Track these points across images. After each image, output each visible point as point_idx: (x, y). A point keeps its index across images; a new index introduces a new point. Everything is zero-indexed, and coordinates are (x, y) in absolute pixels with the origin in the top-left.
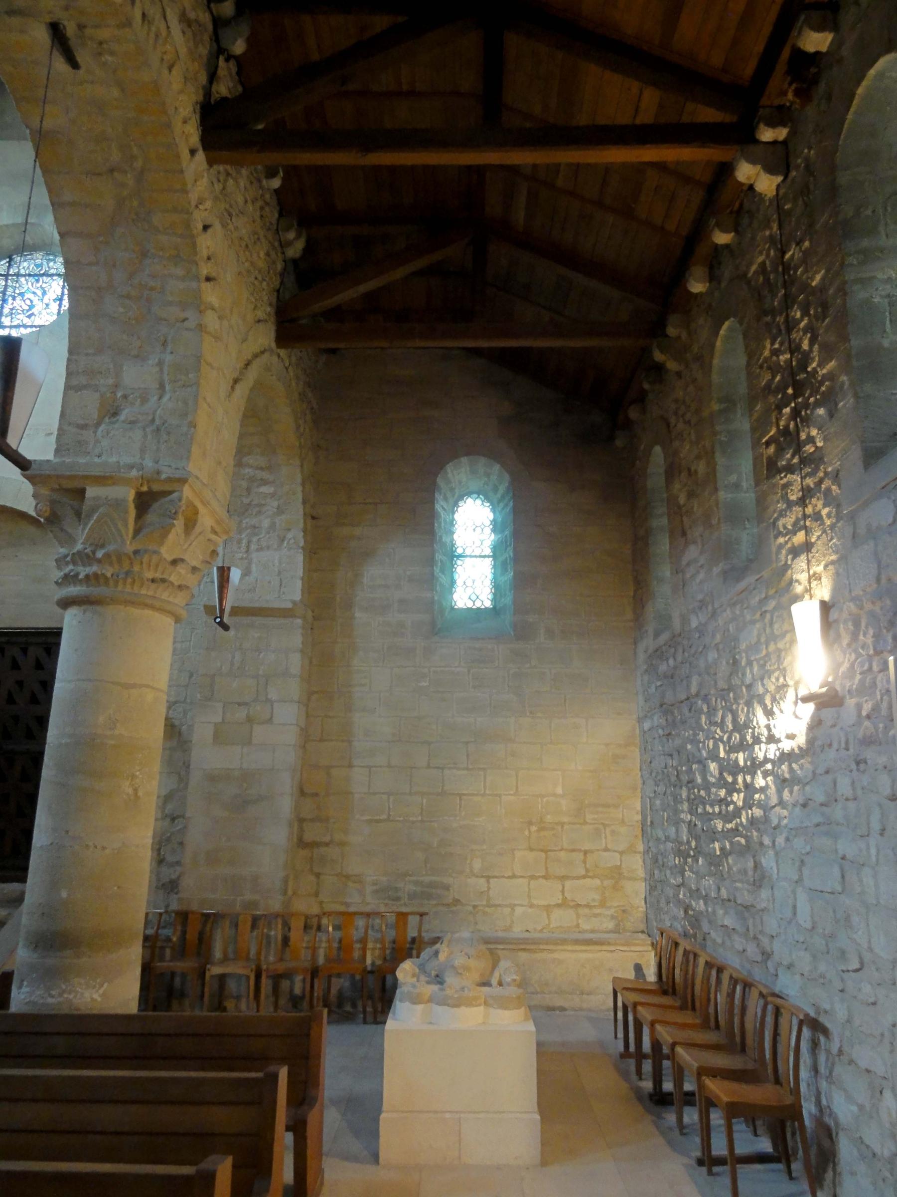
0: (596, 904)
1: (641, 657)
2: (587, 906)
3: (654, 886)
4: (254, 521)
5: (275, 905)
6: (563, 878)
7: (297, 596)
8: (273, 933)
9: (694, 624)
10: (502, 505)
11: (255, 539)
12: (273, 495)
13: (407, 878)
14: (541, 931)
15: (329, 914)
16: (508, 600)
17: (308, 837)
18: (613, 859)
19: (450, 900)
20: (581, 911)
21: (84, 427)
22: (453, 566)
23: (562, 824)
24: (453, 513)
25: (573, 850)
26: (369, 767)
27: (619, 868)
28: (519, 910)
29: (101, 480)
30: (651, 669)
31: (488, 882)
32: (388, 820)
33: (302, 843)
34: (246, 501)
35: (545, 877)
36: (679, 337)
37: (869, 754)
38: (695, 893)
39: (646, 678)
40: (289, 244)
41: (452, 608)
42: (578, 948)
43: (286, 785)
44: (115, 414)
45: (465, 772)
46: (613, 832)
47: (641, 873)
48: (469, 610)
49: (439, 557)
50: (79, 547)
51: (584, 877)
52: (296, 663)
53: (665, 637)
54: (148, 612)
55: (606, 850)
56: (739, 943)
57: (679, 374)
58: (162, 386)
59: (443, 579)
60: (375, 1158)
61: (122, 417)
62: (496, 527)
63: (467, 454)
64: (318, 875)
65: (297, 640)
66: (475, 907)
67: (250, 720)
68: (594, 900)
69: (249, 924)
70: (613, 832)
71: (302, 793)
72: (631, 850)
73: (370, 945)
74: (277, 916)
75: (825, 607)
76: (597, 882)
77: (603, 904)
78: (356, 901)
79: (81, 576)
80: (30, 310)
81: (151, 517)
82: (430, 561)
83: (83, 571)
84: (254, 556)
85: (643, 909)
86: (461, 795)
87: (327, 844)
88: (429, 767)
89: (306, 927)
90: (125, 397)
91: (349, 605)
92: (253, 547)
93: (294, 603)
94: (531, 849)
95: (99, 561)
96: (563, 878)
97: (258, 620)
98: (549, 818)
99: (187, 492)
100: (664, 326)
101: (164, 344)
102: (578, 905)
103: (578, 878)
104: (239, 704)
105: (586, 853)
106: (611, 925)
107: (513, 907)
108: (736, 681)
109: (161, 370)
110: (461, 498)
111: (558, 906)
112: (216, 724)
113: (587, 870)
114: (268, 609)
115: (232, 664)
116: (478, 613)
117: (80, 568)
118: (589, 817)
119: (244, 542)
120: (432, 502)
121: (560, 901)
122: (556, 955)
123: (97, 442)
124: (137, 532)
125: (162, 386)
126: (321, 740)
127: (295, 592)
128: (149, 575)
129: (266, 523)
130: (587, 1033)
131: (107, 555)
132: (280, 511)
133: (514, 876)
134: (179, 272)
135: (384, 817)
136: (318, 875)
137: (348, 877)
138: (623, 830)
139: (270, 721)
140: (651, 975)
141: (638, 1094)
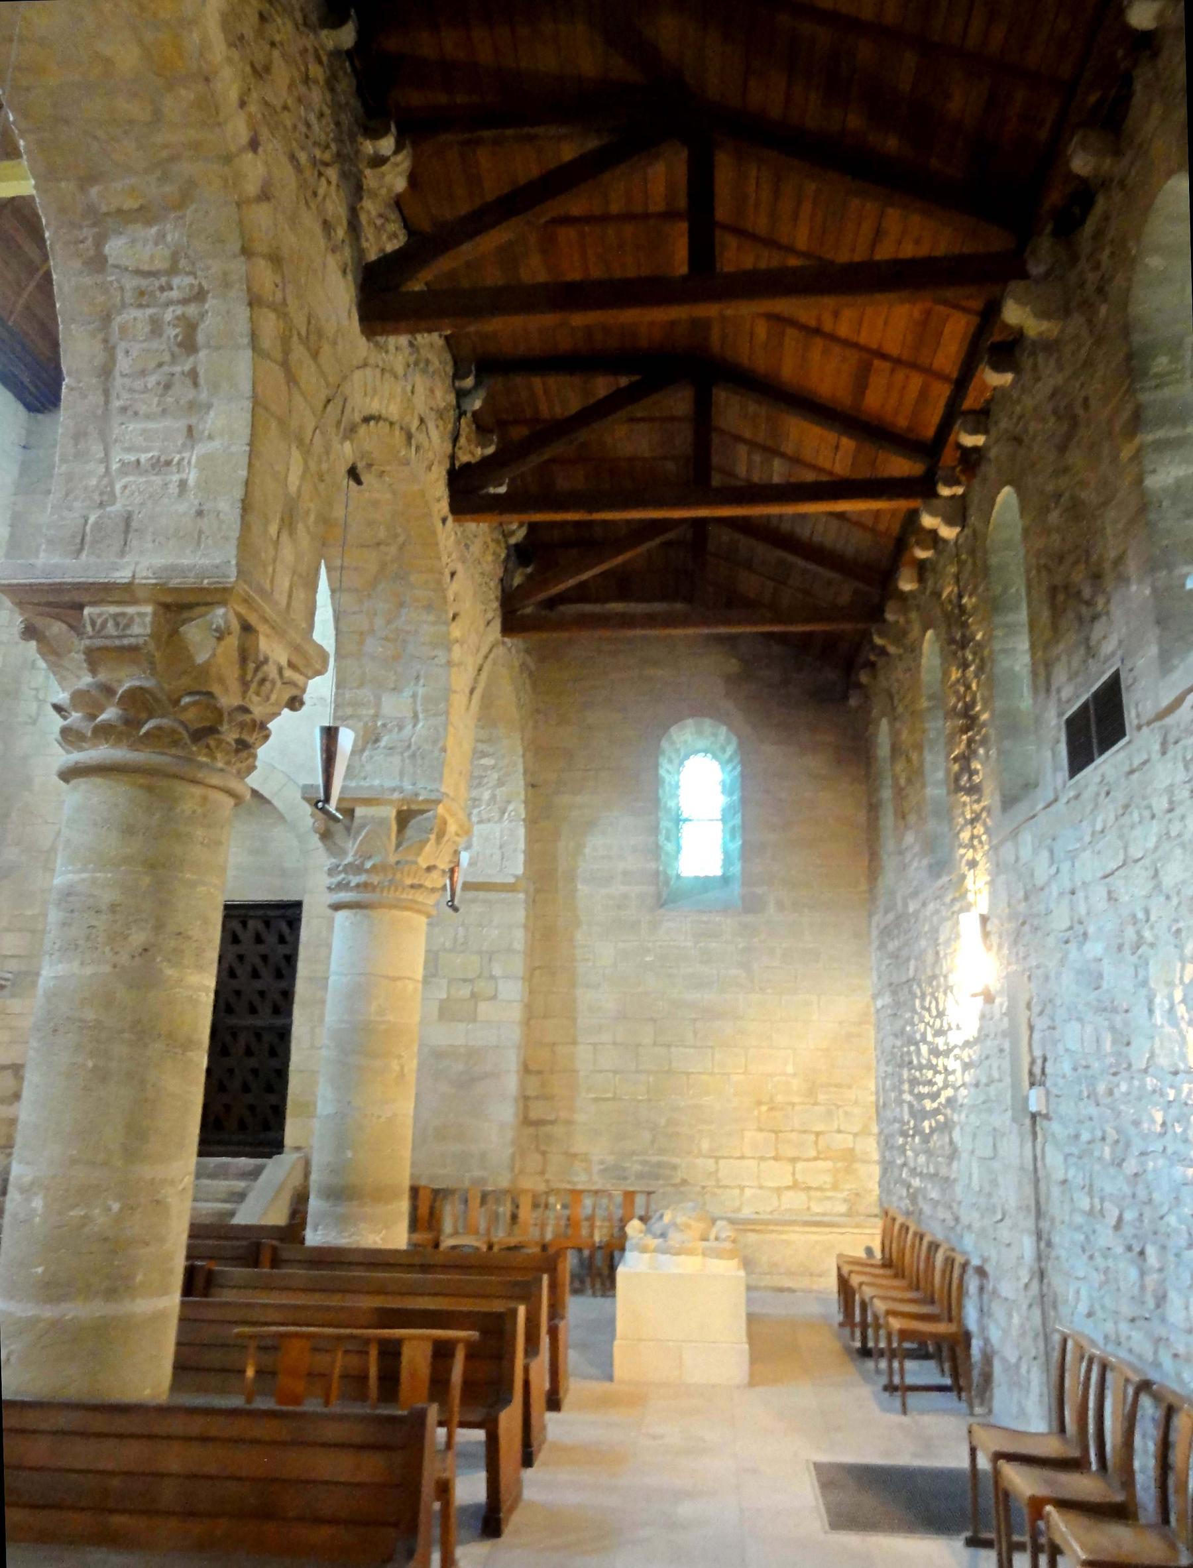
0: (828, 1186)
1: (875, 933)
2: (819, 1189)
3: (886, 1166)
5: (504, 1182)
6: (794, 1160)
7: (520, 870)
8: (501, 1209)
9: (911, 910)
10: (730, 767)
11: (475, 811)
12: (493, 767)
13: (635, 1158)
14: (771, 1212)
15: (556, 1192)
16: (737, 868)
17: (533, 1115)
19: (678, 1181)
20: (813, 1193)
22: (678, 831)
23: (793, 1105)
24: (679, 773)
25: (805, 1132)
26: (595, 1045)
27: (852, 1150)
28: (748, 1192)
29: (367, 802)
30: (882, 946)
31: (717, 1163)
32: (614, 1099)
33: (526, 1121)
35: (776, 1158)
36: (897, 622)
38: (914, 1172)
40: (512, 533)
41: (678, 876)
42: (807, 1229)
43: (511, 1062)
44: (377, 740)
45: (692, 1050)
46: (846, 1113)
47: (876, 1156)
48: (697, 878)
49: (665, 824)
50: (349, 859)
51: (816, 1159)
52: (519, 938)
53: (891, 916)
54: (406, 914)
55: (839, 1131)
56: (942, 1213)
57: (900, 657)
58: (415, 716)
59: (669, 847)
60: (610, 1378)
61: (383, 743)
62: (727, 790)
63: (692, 716)
64: (544, 1153)
65: (520, 915)
66: (704, 1187)
67: (474, 995)
68: (825, 1183)
69: (478, 1200)
70: (846, 1113)
72: (864, 1132)
73: (598, 1223)
74: (506, 1192)
75: (984, 919)
76: (829, 1164)
77: (835, 1187)
78: (581, 1181)
79: (352, 884)
81: (409, 832)
82: (655, 830)
83: (355, 880)
84: (477, 829)
85: (876, 1191)
86: (688, 1074)
87: (552, 1122)
88: (655, 1044)
89: (535, 1206)
90: (384, 725)
91: (571, 877)
93: (516, 877)
94: (760, 1130)
95: (367, 871)
96: (794, 1160)
97: (482, 895)
98: (780, 1098)
99: (440, 809)
100: (882, 611)
101: (418, 678)
102: (809, 1188)
103: (808, 1160)
104: (465, 980)
105: (818, 1134)
106: (843, 1208)
107: (742, 1188)
108: (937, 972)
109: (415, 702)
110: (687, 757)
111: (788, 1188)
112: (442, 1001)
113: (819, 1152)
114: (489, 884)
115: (455, 940)
116: (705, 884)
117: (351, 877)
118: (821, 1098)
120: (656, 766)
121: (791, 1184)
122: (784, 1237)
123: (363, 766)
124: (398, 845)
125: (415, 716)
126: (545, 1017)
127: (517, 866)
128: (408, 882)
129: (486, 795)
130: (814, 1309)
131: (374, 867)
132: (501, 783)
133: (742, 1157)
134: (431, 618)
135: (610, 1095)
136: (544, 1153)
137: (575, 1155)
138: (857, 1111)
139: (494, 997)
140: (878, 1254)
141: (848, 1350)
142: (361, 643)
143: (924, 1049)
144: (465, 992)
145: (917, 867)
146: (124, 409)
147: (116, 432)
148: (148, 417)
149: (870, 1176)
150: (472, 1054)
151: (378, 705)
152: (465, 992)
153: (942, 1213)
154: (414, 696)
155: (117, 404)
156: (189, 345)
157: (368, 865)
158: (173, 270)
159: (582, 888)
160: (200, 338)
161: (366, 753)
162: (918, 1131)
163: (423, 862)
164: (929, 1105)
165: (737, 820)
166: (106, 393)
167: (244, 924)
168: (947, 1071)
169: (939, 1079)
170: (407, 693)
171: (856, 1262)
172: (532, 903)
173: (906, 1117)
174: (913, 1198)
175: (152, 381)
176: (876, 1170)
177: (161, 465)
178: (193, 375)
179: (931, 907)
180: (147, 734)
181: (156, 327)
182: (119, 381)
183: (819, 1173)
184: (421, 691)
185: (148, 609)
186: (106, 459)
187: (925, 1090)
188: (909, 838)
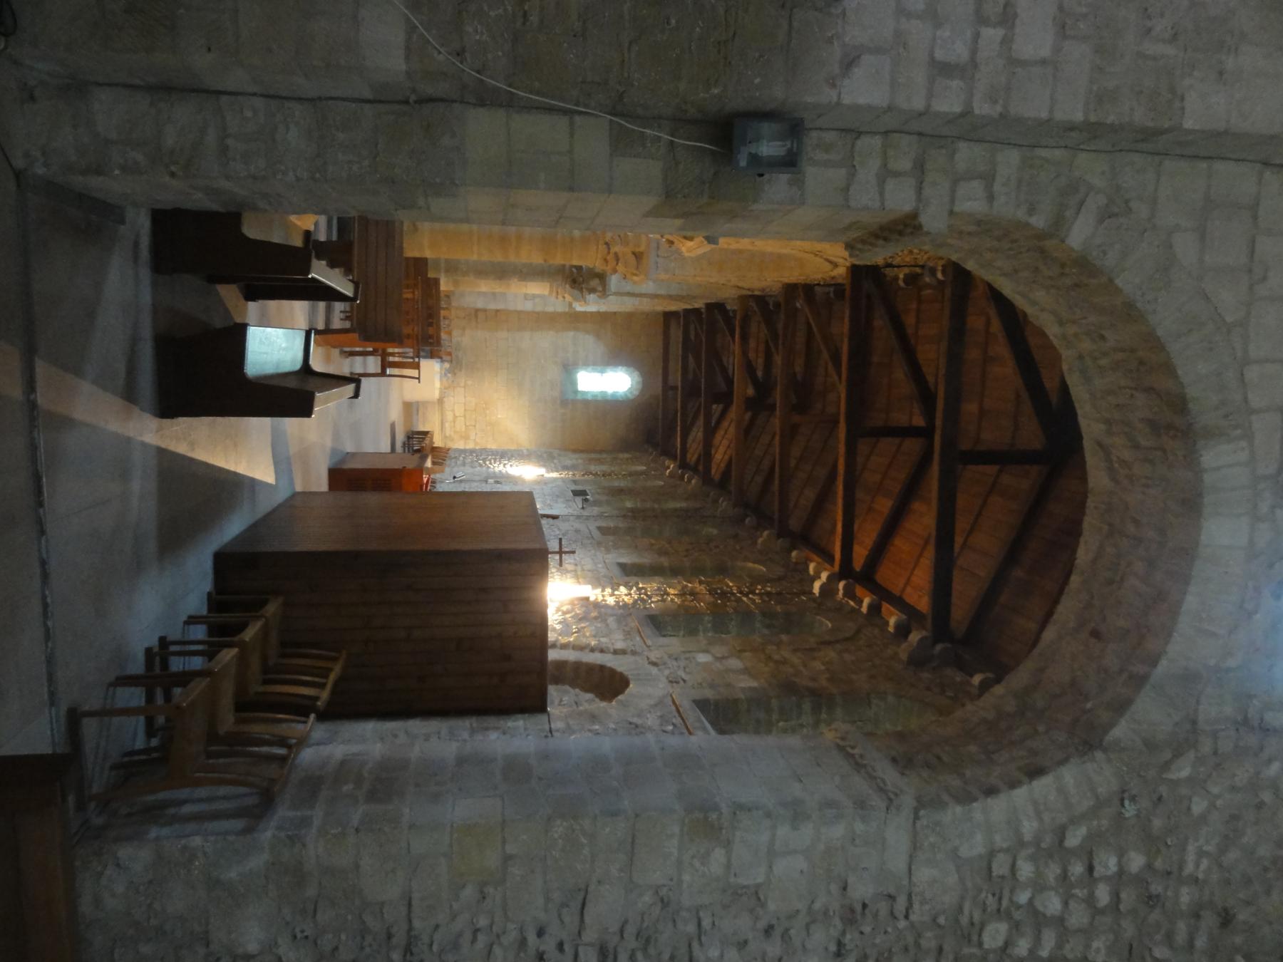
3: (464, 451)
5: (454, 304)
6: (465, 416)
16: (579, 397)
18: (473, 437)
19: (456, 371)
23: (486, 417)
33: (477, 310)
35: (465, 410)
43: (500, 306)
47: (467, 447)
49: (599, 368)
52: (550, 309)
53: (556, 455)
55: (476, 434)
62: (614, 394)
63: (643, 381)
64: (464, 318)
71: (497, 311)
72: (476, 443)
74: (450, 304)
75: (543, 475)
76: (463, 430)
77: (455, 432)
78: (455, 333)
91: (576, 329)
96: (465, 416)
98: (488, 412)
102: (454, 422)
105: (475, 426)
106: (447, 434)
107: (453, 397)
111: (454, 415)
116: (574, 383)
118: (489, 428)
128: (559, 291)
136: (464, 318)
143: (506, 462)
145: (568, 462)
149: (460, 445)
153: (453, 464)
159: (571, 334)
162: (479, 459)
163: (566, 295)
164: (488, 463)
165: (599, 398)
168: (498, 467)
169: (496, 465)
171: (432, 438)
172: (565, 314)
173: (483, 457)
174: (455, 458)
176: (462, 447)
179: (553, 465)
180: (572, 271)
183: (460, 425)
187: (493, 461)
188: (580, 461)
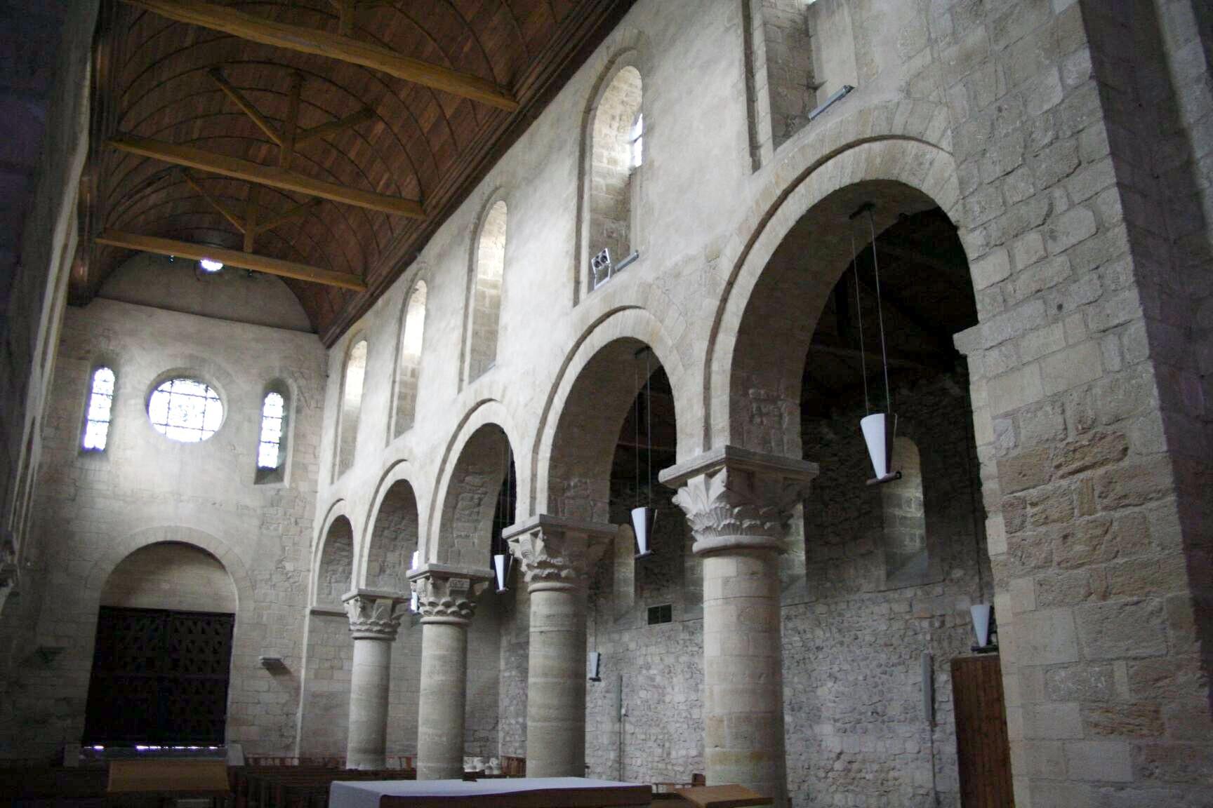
4: (335, 567)
11: (334, 577)
21: (375, 576)
34: (332, 558)
37: (607, 695)
39: (508, 654)
44: (384, 571)
50: (373, 620)
58: (400, 564)
67: (332, 668)
80: (186, 415)
83: (376, 628)
84: (333, 585)
92: (333, 580)
95: (380, 625)
119: (328, 578)
129: (341, 569)
139: (341, 668)
142: (383, 531)
144: (327, 665)
146: (457, 519)
147: (455, 525)
148: (465, 522)
150: (332, 695)
151: (386, 557)
152: (327, 665)
154: (400, 555)
155: (456, 517)
156: (479, 505)
157: (381, 622)
158: (482, 486)
160: (482, 503)
161: (380, 577)
166: (454, 513)
167: (195, 623)
170: (397, 553)
175: (467, 512)
177: (467, 536)
178: (478, 513)
181: (472, 499)
182: (457, 510)
184: (403, 552)
185: (468, 580)
186: (452, 533)
